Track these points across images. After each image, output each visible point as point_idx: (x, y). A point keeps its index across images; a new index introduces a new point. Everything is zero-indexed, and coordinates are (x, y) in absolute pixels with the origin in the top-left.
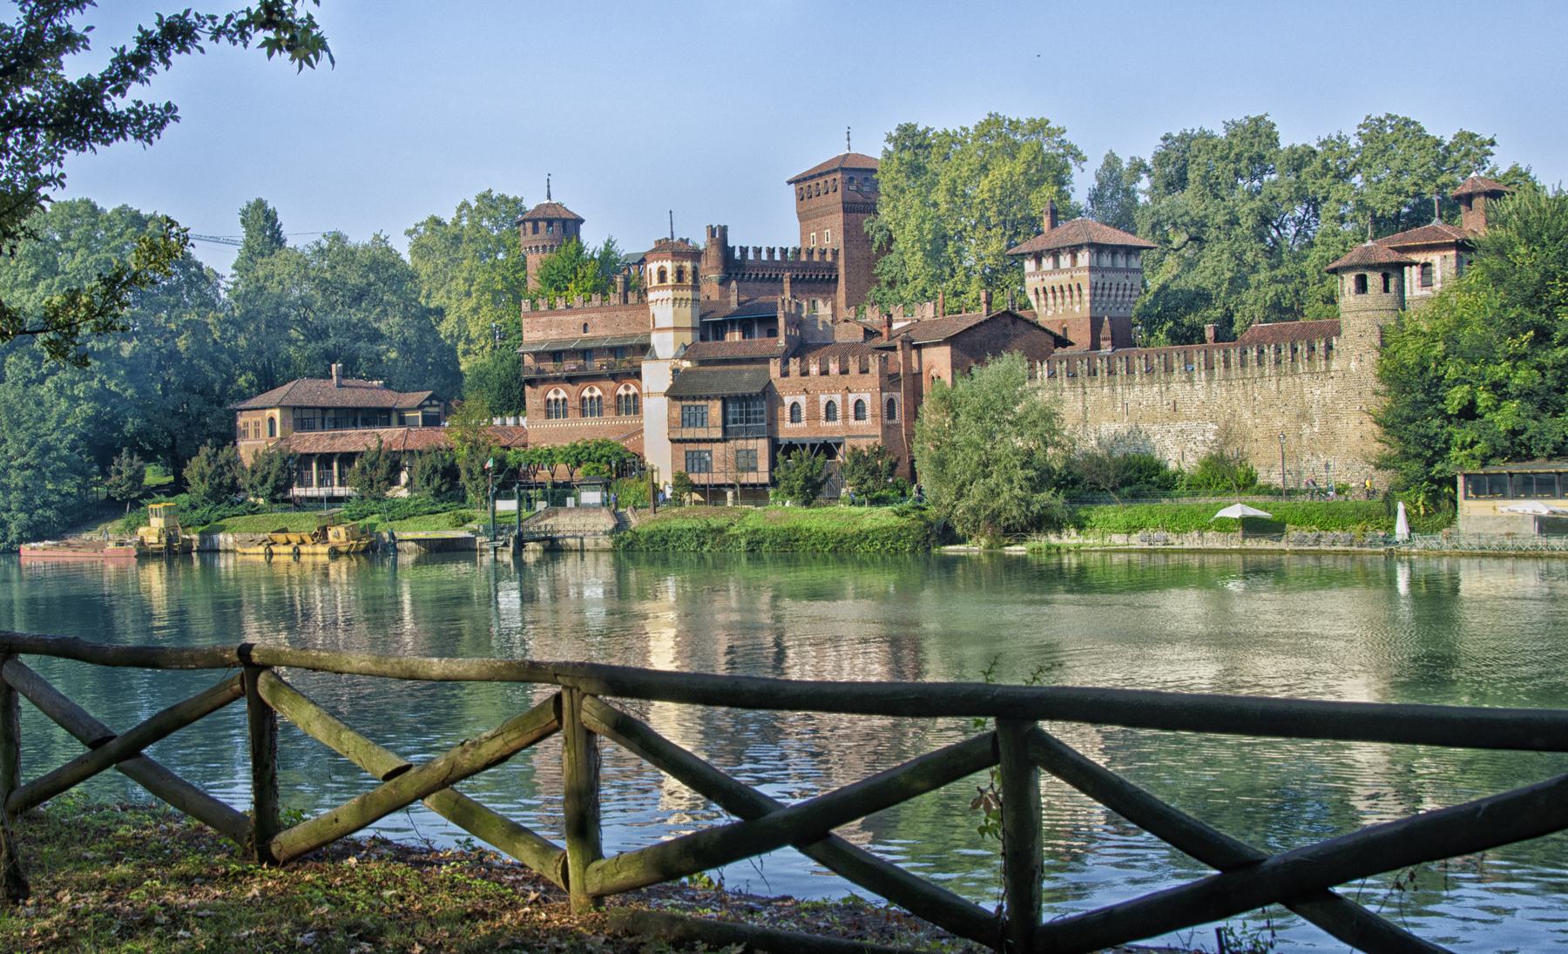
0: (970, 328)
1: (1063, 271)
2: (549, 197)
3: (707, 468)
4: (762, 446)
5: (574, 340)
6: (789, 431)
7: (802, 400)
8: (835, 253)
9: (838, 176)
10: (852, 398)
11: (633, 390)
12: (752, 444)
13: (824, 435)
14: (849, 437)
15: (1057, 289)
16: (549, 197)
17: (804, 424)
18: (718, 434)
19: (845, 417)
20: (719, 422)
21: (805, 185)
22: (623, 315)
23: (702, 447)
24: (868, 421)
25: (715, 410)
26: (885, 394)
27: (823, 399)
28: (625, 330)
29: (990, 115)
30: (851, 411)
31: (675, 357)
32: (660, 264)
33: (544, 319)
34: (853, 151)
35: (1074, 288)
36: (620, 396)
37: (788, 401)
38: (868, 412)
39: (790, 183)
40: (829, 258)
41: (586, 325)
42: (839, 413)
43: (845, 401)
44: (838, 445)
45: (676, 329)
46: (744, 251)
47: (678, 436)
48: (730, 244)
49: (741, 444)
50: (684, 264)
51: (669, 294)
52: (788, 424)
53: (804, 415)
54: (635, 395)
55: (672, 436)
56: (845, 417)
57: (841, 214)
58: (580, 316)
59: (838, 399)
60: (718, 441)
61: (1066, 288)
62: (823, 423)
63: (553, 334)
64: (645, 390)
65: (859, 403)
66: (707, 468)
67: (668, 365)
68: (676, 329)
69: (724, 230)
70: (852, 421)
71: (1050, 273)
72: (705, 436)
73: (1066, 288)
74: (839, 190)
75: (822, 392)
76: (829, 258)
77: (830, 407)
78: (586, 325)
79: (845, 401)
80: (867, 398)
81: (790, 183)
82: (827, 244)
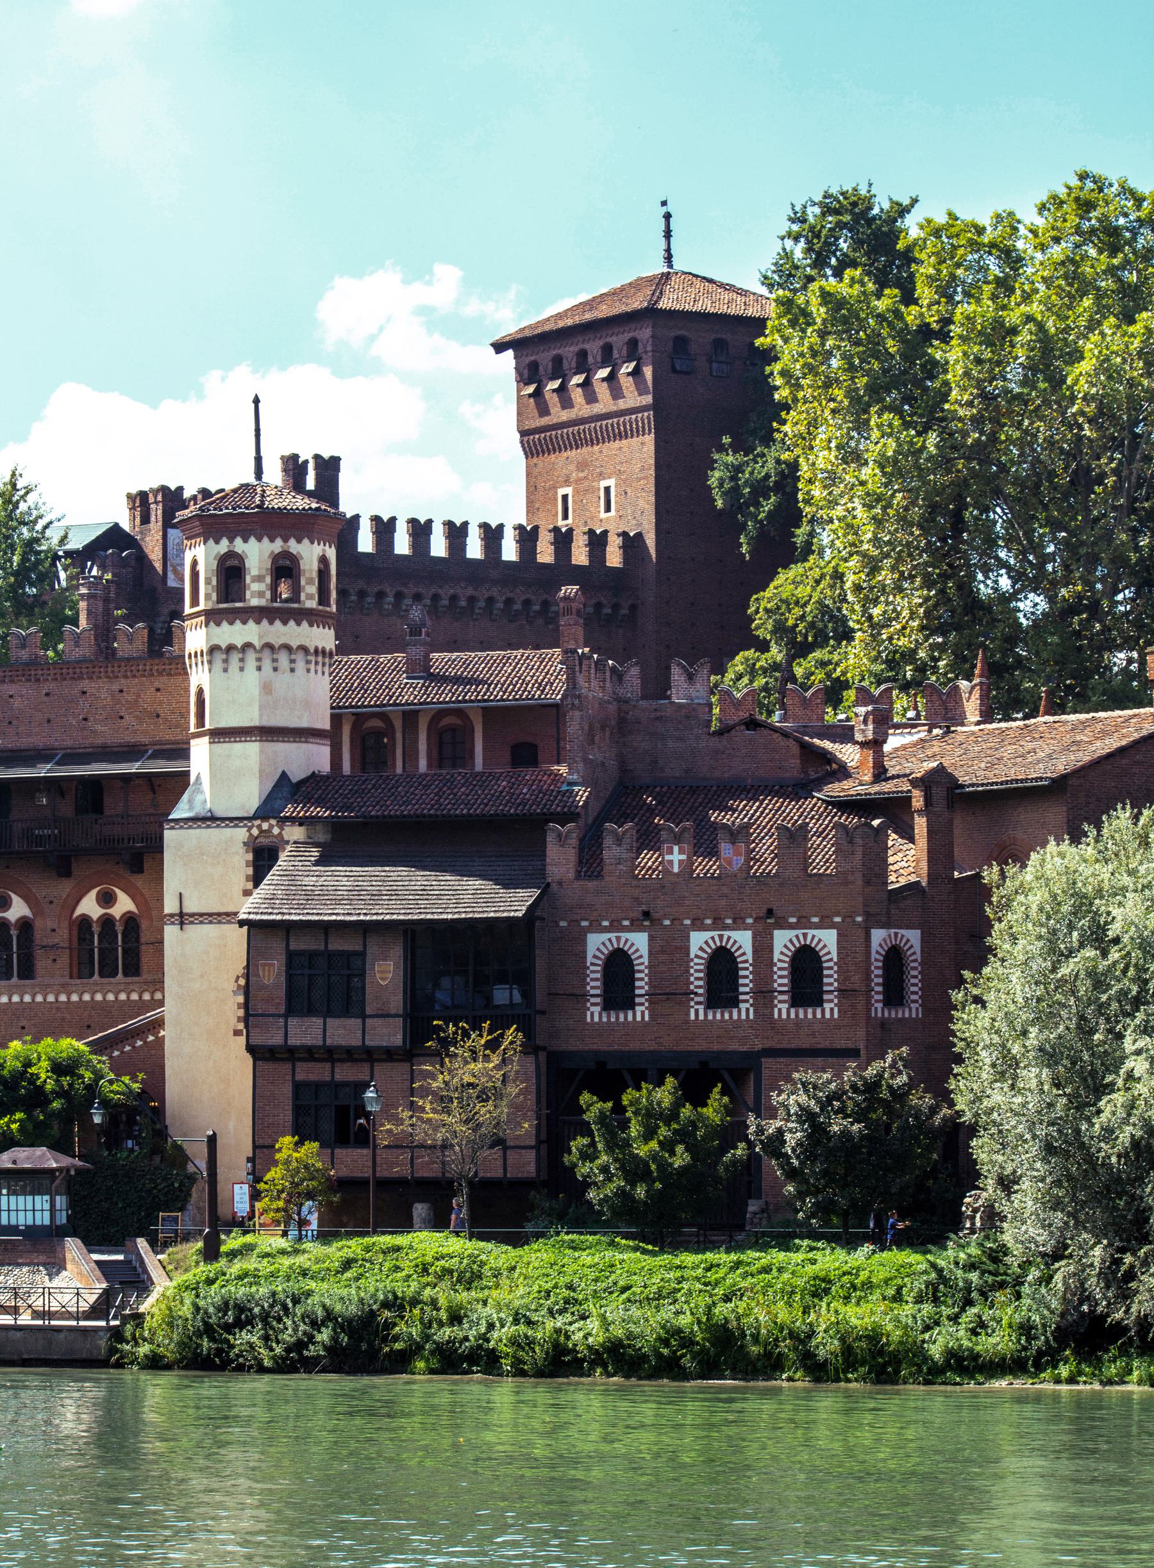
0: (1121, 750)
6: (600, 1030)
7: (639, 943)
8: (632, 544)
9: (644, 333)
10: (783, 941)
11: (124, 904)
13: (700, 1045)
17: (641, 1012)
18: (390, 1034)
19: (763, 994)
20: (396, 1002)
21: (545, 358)
22: (101, 690)
23: (345, 1073)
24: (830, 1008)
26: (878, 936)
27: (700, 941)
29: (1083, 176)
30: (781, 980)
31: (266, 811)
32: (224, 546)
36: (85, 920)
37: (597, 944)
38: (831, 980)
39: (499, 347)
40: (614, 557)
42: (746, 983)
43: (763, 948)
45: (267, 733)
46: (384, 529)
47: (275, 1039)
48: (347, 507)
50: (293, 546)
52: (594, 1013)
53: (642, 985)
54: (130, 920)
55: (258, 1040)
56: (763, 994)
57: (649, 439)
59: (742, 940)
60: (389, 1055)
62: (697, 1012)
64: (170, 906)
68: (267, 733)
69: (329, 468)
70: (782, 1009)
72: (355, 1041)
75: (697, 924)
76: (614, 557)
79: (763, 948)
80: (827, 940)
81: (499, 347)
82: (608, 521)
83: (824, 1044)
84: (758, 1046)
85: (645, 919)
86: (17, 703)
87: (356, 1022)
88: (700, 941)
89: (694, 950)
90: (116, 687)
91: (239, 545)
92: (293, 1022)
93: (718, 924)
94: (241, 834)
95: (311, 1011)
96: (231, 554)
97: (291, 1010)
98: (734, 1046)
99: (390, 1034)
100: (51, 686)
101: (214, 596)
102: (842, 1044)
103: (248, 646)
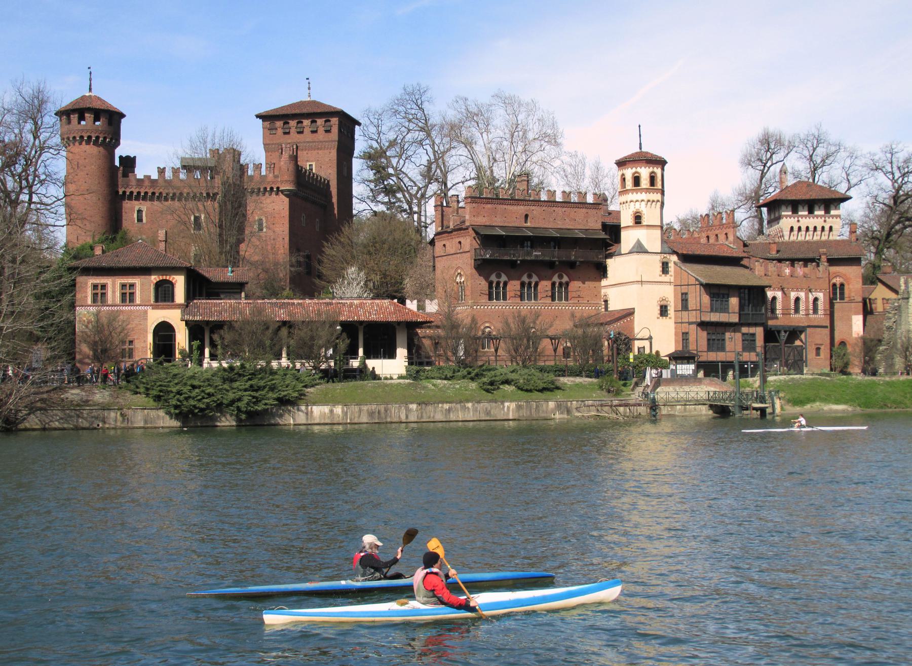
1: (817, 216)
2: (90, 90)
3: (722, 349)
4: (759, 332)
5: (518, 228)
12: (752, 330)
13: (793, 324)
14: (809, 326)
15: (811, 228)
16: (90, 90)
20: (737, 309)
25: (734, 301)
27: (793, 295)
28: (560, 225)
30: (811, 307)
32: (651, 169)
33: (489, 206)
34: (312, 99)
35: (827, 228)
39: (258, 116)
41: (526, 216)
43: (807, 298)
44: (801, 332)
49: (745, 330)
51: (644, 196)
56: (807, 309)
58: (522, 207)
59: (802, 295)
61: (819, 228)
63: (498, 221)
65: (816, 300)
66: (722, 349)
67: (658, 258)
71: (805, 217)
73: (819, 228)
74: (335, 130)
75: (793, 290)
77: (797, 300)
78: (526, 216)
80: (820, 295)
81: (258, 116)
83: (821, 324)
84: (806, 324)
85: (782, 289)
86: (535, 212)
87: (727, 314)
88: (793, 295)
89: (792, 298)
90: (564, 209)
91: (655, 170)
92: (712, 314)
93: (797, 290)
94: (658, 258)
95: (716, 311)
96: (653, 172)
97: (712, 311)
98: (801, 325)
99: (735, 319)
100: (544, 208)
101: (649, 184)
102: (824, 325)
103: (642, 201)
